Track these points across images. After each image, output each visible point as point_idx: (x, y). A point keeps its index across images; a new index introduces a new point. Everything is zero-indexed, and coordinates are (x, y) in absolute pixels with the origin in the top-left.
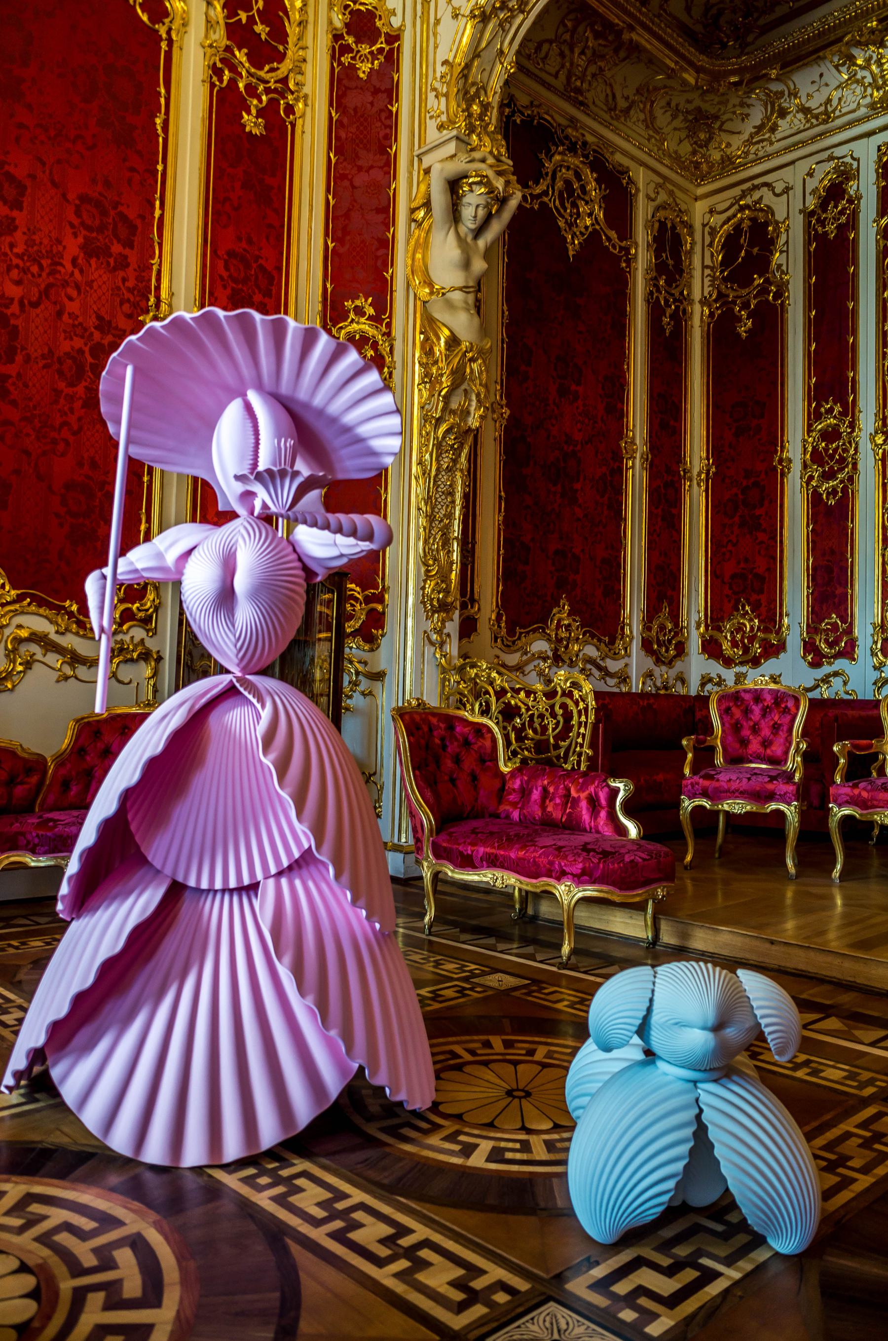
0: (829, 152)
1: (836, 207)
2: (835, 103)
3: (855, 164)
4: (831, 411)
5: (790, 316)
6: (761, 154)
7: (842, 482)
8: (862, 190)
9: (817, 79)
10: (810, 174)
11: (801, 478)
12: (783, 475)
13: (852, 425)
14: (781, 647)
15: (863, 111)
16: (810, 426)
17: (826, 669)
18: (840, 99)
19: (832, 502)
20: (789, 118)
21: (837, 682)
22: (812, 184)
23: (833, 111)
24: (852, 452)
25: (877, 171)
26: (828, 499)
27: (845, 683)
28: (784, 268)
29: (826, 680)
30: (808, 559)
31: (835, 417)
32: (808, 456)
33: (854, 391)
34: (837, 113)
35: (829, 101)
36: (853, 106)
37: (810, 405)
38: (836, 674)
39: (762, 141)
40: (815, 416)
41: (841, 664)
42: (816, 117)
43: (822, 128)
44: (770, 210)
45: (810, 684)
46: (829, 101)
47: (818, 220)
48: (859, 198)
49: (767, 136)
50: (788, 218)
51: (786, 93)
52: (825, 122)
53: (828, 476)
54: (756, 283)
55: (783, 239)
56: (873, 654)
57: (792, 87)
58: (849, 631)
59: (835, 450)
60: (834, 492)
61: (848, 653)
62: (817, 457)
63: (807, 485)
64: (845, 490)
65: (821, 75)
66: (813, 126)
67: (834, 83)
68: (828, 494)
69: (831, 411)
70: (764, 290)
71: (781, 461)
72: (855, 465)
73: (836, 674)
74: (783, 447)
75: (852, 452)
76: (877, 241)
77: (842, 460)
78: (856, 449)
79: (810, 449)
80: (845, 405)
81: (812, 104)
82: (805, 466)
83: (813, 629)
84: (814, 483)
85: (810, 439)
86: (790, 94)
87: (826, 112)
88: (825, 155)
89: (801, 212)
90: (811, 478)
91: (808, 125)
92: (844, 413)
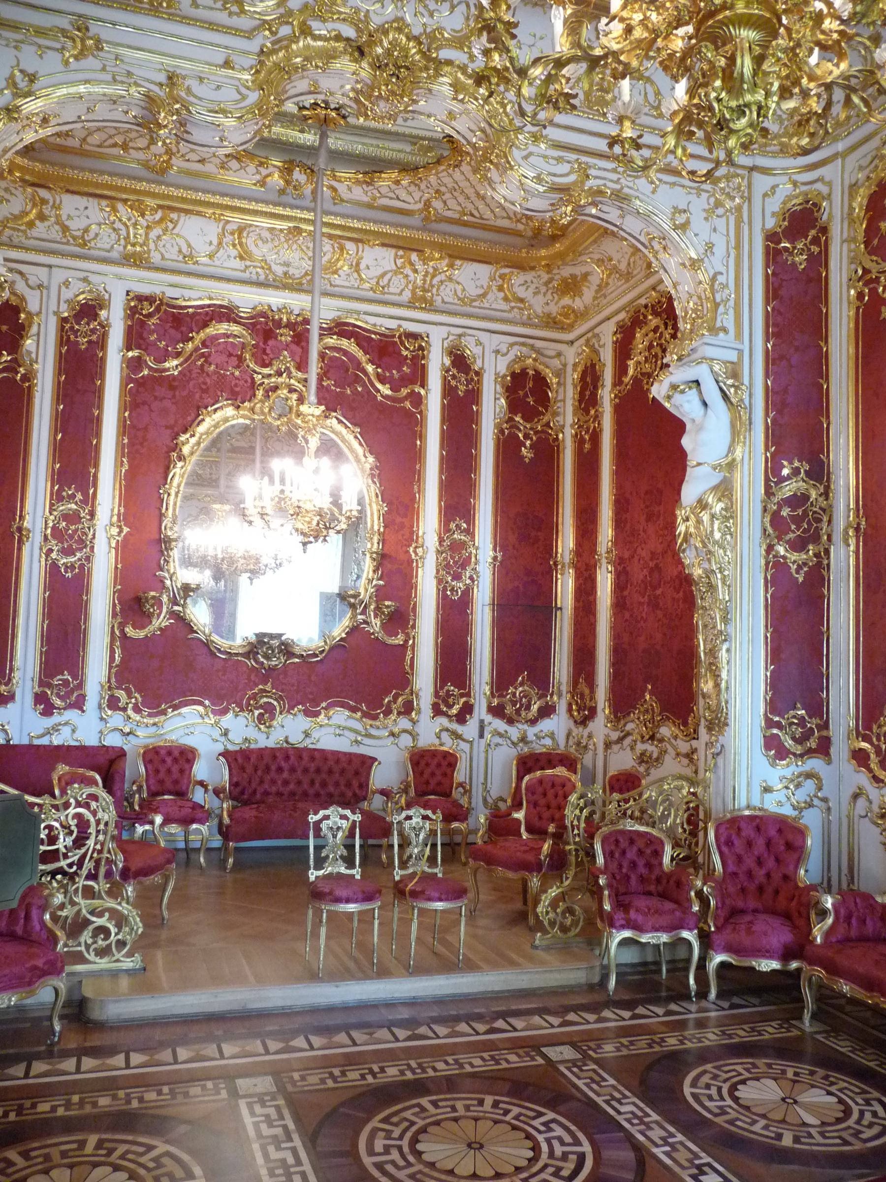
0: (86, 274)
1: (88, 324)
2: (92, 235)
3: (107, 297)
4: (73, 496)
5: (37, 401)
6: (16, 241)
7: (80, 560)
8: (111, 321)
9: (82, 209)
10: (67, 283)
11: (41, 549)
12: (20, 542)
13: (92, 514)
14: (11, 698)
15: (114, 255)
16: (51, 505)
17: (56, 719)
18: (97, 235)
19: (69, 575)
20: (46, 223)
21: (66, 731)
22: (67, 294)
23: (89, 241)
24: (90, 536)
25: (125, 310)
26: (66, 572)
27: (74, 731)
28: (34, 356)
29: (56, 729)
30: (43, 621)
31: (76, 503)
32: (49, 531)
33: (95, 485)
34: (93, 244)
35: (86, 230)
36: (108, 246)
37: (52, 487)
38: (66, 724)
39: (18, 230)
40: (57, 498)
41: (72, 715)
42: (75, 238)
43: (77, 249)
44: (23, 299)
45: (41, 731)
46: (86, 230)
47: (72, 328)
48: (109, 325)
49: (23, 228)
50: (40, 312)
51: (51, 203)
52: (79, 245)
53: (68, 552)
54: (4, 359)
55: (34, 330)
56: (100, 707)
57: (58, 202)
58: (81, 686)
59: (77, 530)
60: (73, 567)
61: (79, 704)
62: (57, 533)
63: (48, 554)
64: (82, 567)
65: (86, 208)
66: (68, 243)
67: (93, 219)
68: (67, 567)
69: (73, 496)
70: (12, 367)
71: (20, 529)
72: (92, 548)
73: (66, 724)
74: (22, 517)
75: (90, 536)
76: (122, 368)
77: (81, 541)
78: (94, 535)
79: (51, 524)
80: (85, 494)
81: (72, 225)
82: (46, 538)
83: (41, 684)
84: (54, 555)
85: (52, 517)
86: (53, 206)
87: (83, 237)
88: (82, 275)
89: (55, 313)
90: (51, 551)
91: (64, 240)
92: (85, 501)
